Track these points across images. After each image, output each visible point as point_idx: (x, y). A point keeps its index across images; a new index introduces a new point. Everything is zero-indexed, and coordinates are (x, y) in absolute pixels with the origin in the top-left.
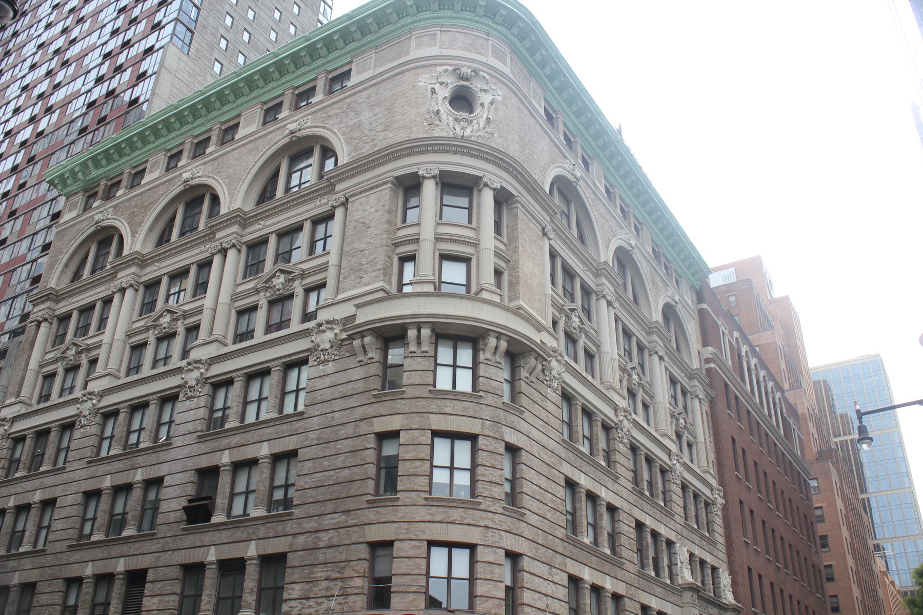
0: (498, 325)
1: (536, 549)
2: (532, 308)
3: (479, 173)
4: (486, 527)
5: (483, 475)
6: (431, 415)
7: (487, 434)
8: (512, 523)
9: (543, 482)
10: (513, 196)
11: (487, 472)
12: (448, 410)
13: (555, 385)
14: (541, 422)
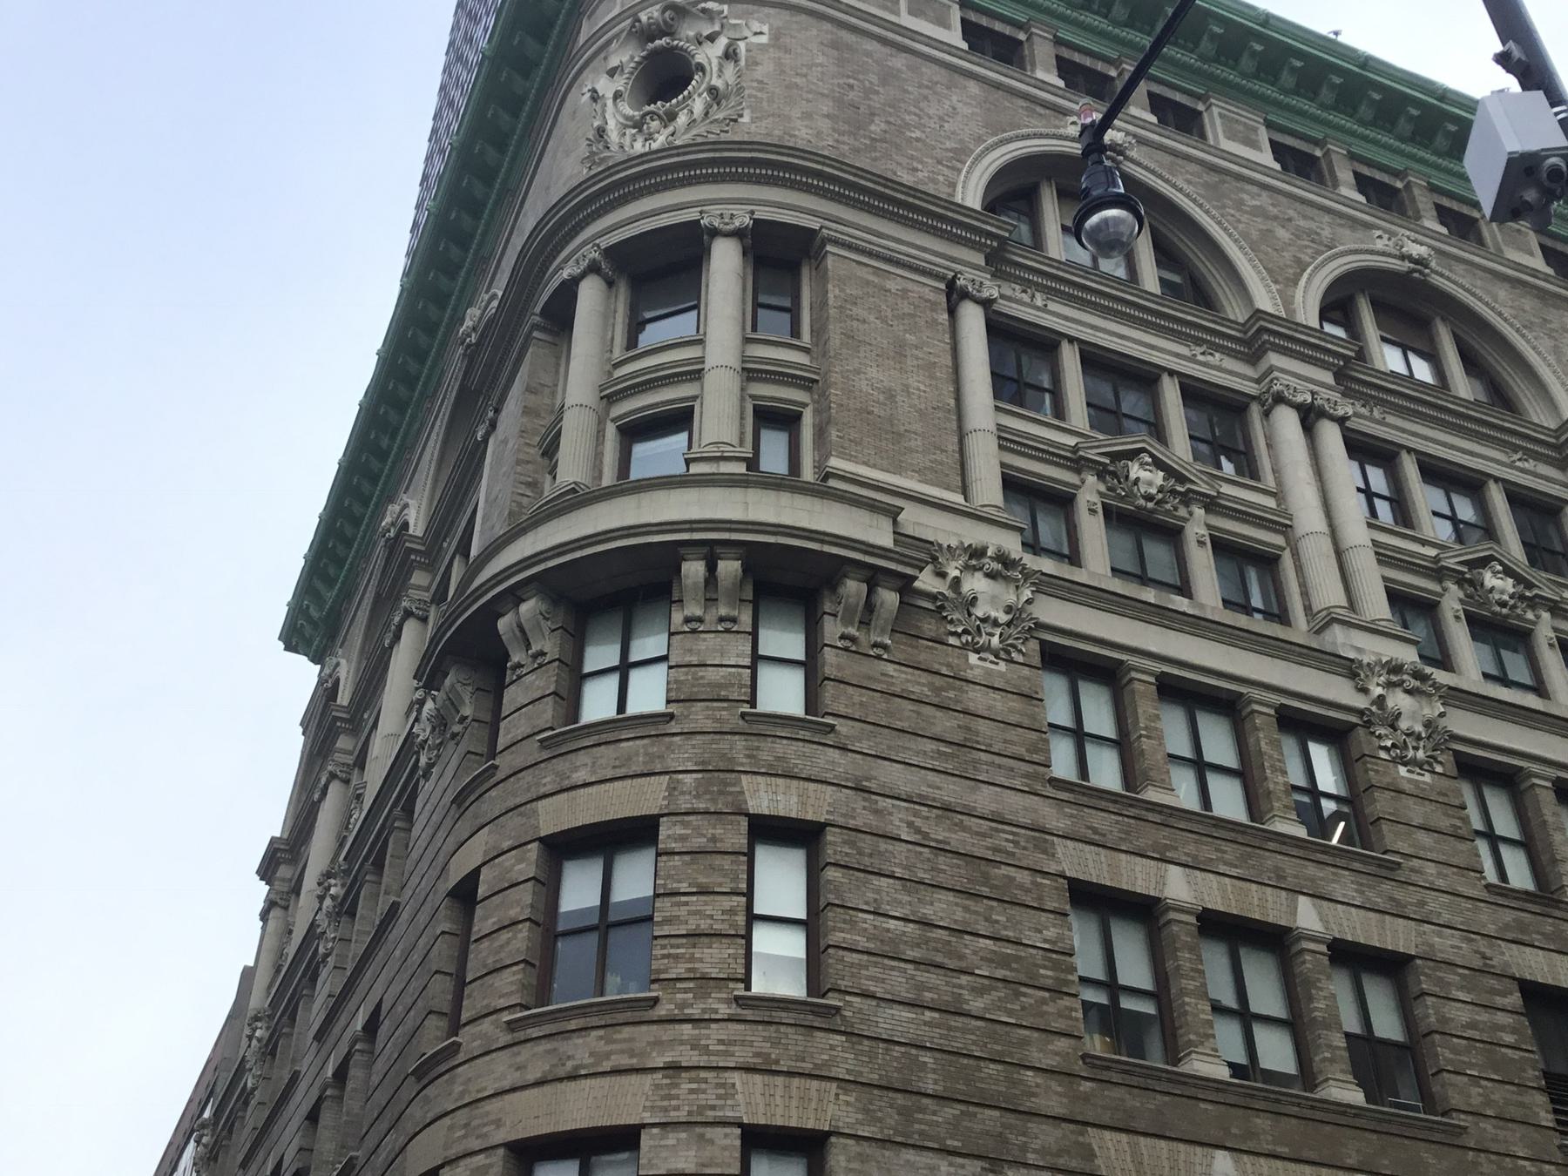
0: (692, 525)
1: (904, 1112)
2: (898, 469)
3: (690, 215)
4: (674, 1068)
5: (668, 921)
6: (541, 804)
7: (685, 807)
8: (776, 1043)
9: (941, 908)
10: (812, 233)
11: (683, 911)
12: (581, 776)
13: (995, 641)
14: (930, 746)
